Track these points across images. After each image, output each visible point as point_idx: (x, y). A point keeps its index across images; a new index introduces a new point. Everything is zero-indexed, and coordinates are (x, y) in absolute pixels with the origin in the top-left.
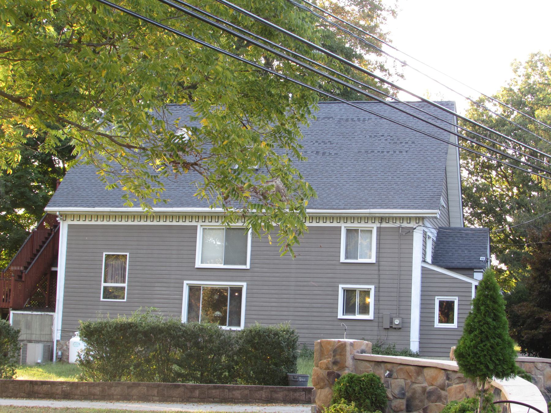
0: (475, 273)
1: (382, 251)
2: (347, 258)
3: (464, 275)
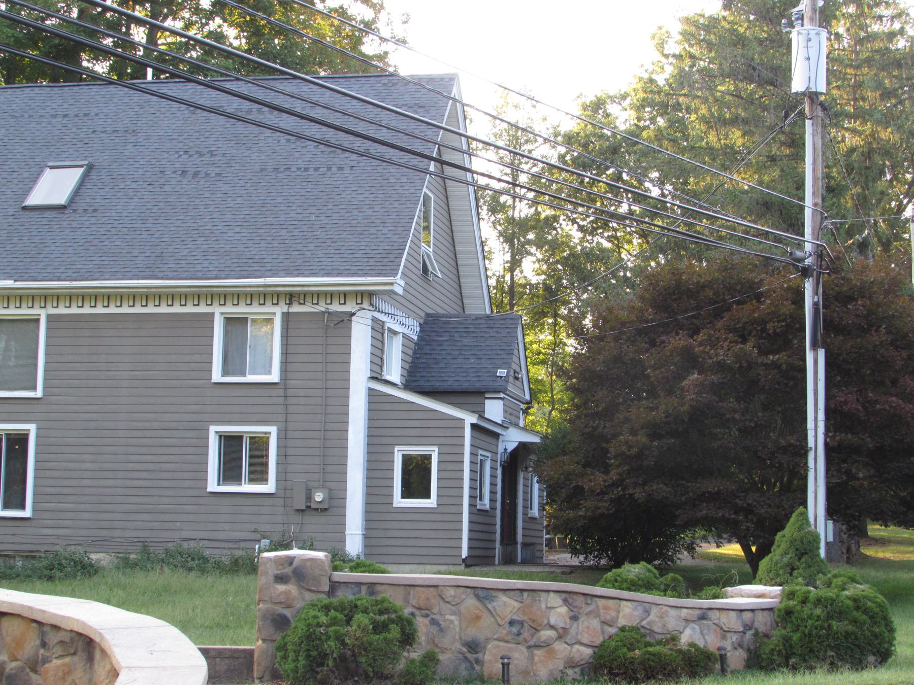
0: (487, 401)
1: (291, 358)
2: (225, 373)
3: (449, 404)
